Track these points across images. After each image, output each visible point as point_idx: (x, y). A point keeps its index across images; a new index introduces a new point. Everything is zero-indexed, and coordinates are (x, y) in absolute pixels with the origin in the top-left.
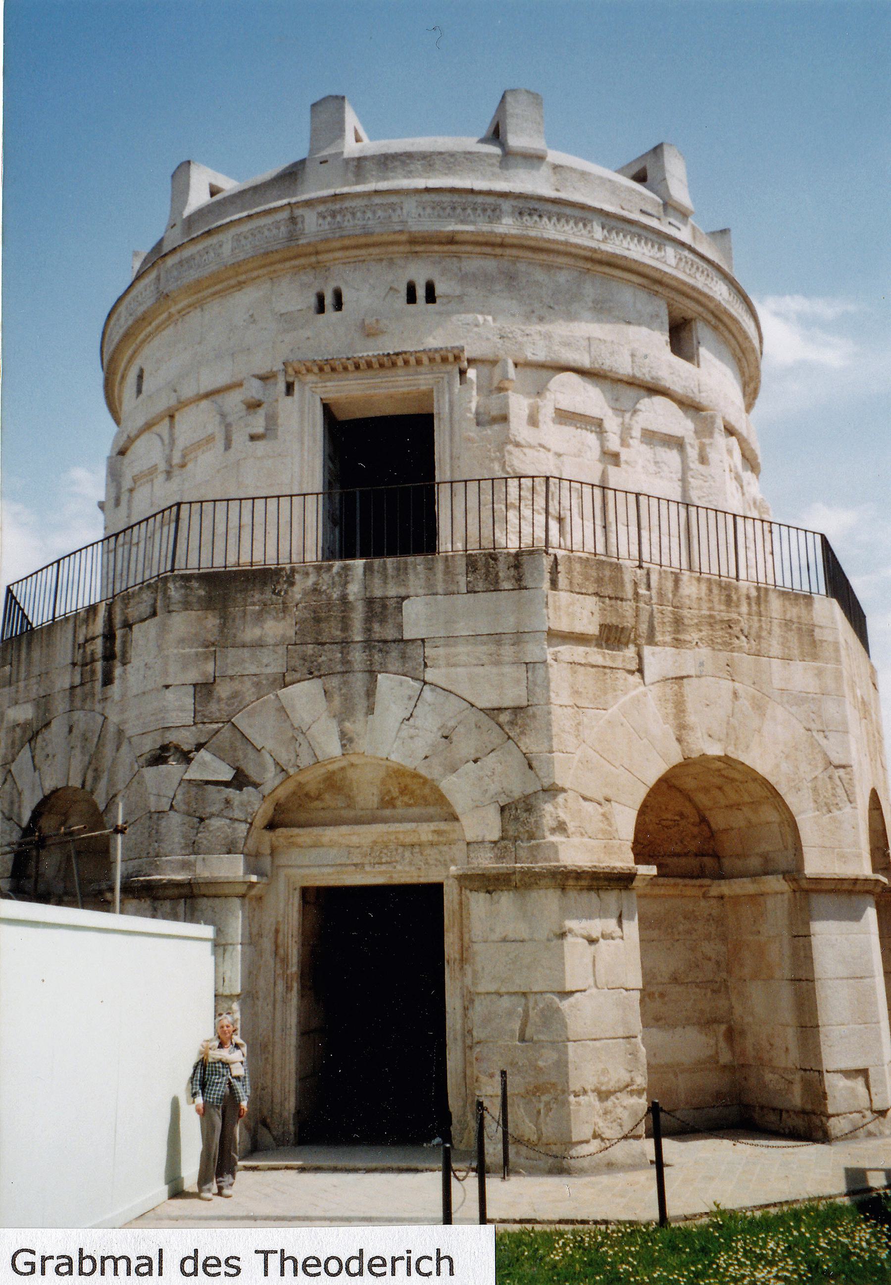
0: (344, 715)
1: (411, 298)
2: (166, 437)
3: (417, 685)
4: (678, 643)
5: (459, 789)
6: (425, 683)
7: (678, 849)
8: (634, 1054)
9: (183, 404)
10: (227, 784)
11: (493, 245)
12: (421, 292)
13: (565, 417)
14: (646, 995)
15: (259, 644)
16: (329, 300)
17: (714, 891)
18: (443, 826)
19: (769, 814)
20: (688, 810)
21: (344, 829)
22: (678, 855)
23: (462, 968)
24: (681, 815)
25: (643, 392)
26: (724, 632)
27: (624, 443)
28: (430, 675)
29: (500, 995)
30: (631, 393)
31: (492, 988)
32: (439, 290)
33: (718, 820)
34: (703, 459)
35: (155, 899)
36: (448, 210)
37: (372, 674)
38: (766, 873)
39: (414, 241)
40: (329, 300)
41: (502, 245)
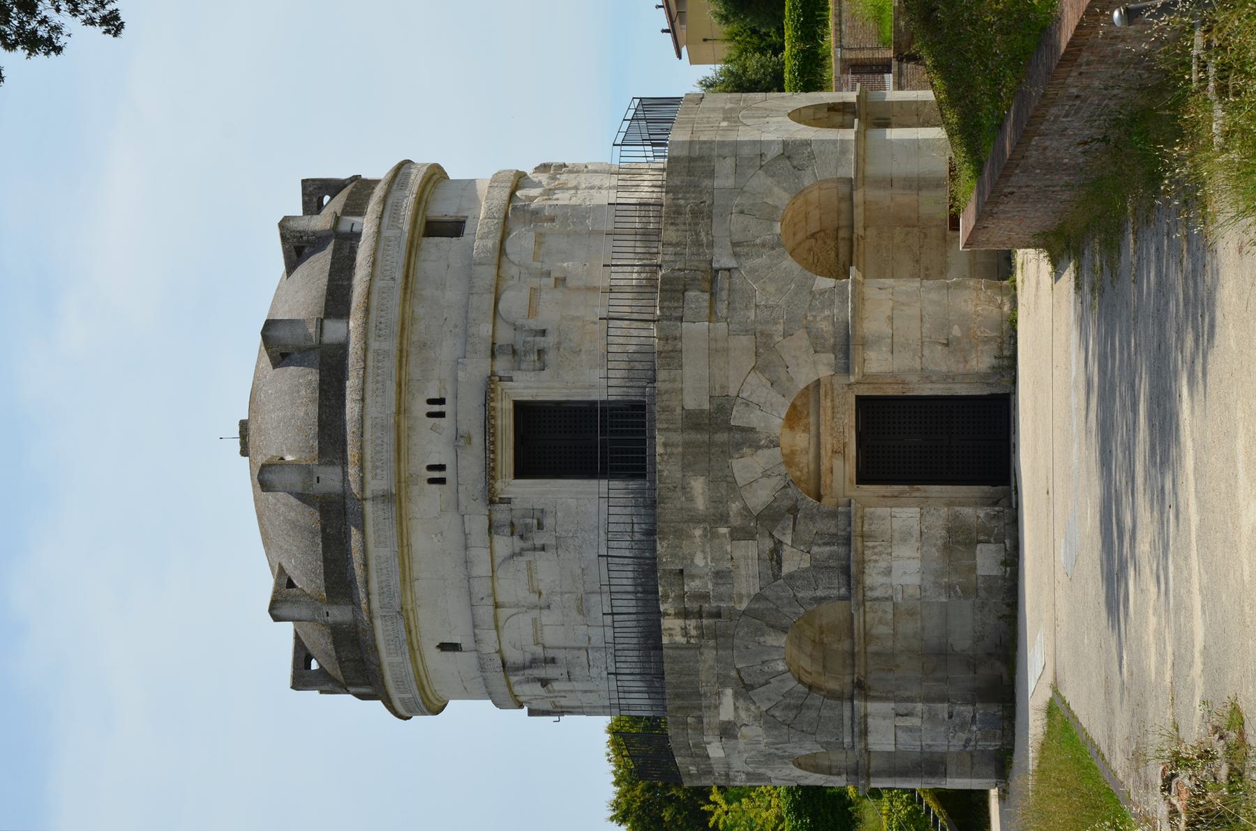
1: (441, 415)
4: (711, 245)
5: (803, 378)
7: (833, 254)
8: (957, 285)
9: (493, 594)
10: (795, 519)
11: (401, 357)
13: (532, 310)
14: (927, 277)
16: (436, 475)
17: (861, 232)
20: (807, 244)
21: (823, 452)
22: (837, 256)
24: (810, 250)
25: (504, 259)
26: (702, 214)
27: (548, 274)
28: (733, 393)
30: (505, 266)
31: (918, 360)
32: (435, 395)
33: (814, 227)
34: (552, 219)
35: (864, 562)
37: (731, 429)
38: (852, 199)
39: (398, 412)
40: (436, 475)
41: (401, 351)
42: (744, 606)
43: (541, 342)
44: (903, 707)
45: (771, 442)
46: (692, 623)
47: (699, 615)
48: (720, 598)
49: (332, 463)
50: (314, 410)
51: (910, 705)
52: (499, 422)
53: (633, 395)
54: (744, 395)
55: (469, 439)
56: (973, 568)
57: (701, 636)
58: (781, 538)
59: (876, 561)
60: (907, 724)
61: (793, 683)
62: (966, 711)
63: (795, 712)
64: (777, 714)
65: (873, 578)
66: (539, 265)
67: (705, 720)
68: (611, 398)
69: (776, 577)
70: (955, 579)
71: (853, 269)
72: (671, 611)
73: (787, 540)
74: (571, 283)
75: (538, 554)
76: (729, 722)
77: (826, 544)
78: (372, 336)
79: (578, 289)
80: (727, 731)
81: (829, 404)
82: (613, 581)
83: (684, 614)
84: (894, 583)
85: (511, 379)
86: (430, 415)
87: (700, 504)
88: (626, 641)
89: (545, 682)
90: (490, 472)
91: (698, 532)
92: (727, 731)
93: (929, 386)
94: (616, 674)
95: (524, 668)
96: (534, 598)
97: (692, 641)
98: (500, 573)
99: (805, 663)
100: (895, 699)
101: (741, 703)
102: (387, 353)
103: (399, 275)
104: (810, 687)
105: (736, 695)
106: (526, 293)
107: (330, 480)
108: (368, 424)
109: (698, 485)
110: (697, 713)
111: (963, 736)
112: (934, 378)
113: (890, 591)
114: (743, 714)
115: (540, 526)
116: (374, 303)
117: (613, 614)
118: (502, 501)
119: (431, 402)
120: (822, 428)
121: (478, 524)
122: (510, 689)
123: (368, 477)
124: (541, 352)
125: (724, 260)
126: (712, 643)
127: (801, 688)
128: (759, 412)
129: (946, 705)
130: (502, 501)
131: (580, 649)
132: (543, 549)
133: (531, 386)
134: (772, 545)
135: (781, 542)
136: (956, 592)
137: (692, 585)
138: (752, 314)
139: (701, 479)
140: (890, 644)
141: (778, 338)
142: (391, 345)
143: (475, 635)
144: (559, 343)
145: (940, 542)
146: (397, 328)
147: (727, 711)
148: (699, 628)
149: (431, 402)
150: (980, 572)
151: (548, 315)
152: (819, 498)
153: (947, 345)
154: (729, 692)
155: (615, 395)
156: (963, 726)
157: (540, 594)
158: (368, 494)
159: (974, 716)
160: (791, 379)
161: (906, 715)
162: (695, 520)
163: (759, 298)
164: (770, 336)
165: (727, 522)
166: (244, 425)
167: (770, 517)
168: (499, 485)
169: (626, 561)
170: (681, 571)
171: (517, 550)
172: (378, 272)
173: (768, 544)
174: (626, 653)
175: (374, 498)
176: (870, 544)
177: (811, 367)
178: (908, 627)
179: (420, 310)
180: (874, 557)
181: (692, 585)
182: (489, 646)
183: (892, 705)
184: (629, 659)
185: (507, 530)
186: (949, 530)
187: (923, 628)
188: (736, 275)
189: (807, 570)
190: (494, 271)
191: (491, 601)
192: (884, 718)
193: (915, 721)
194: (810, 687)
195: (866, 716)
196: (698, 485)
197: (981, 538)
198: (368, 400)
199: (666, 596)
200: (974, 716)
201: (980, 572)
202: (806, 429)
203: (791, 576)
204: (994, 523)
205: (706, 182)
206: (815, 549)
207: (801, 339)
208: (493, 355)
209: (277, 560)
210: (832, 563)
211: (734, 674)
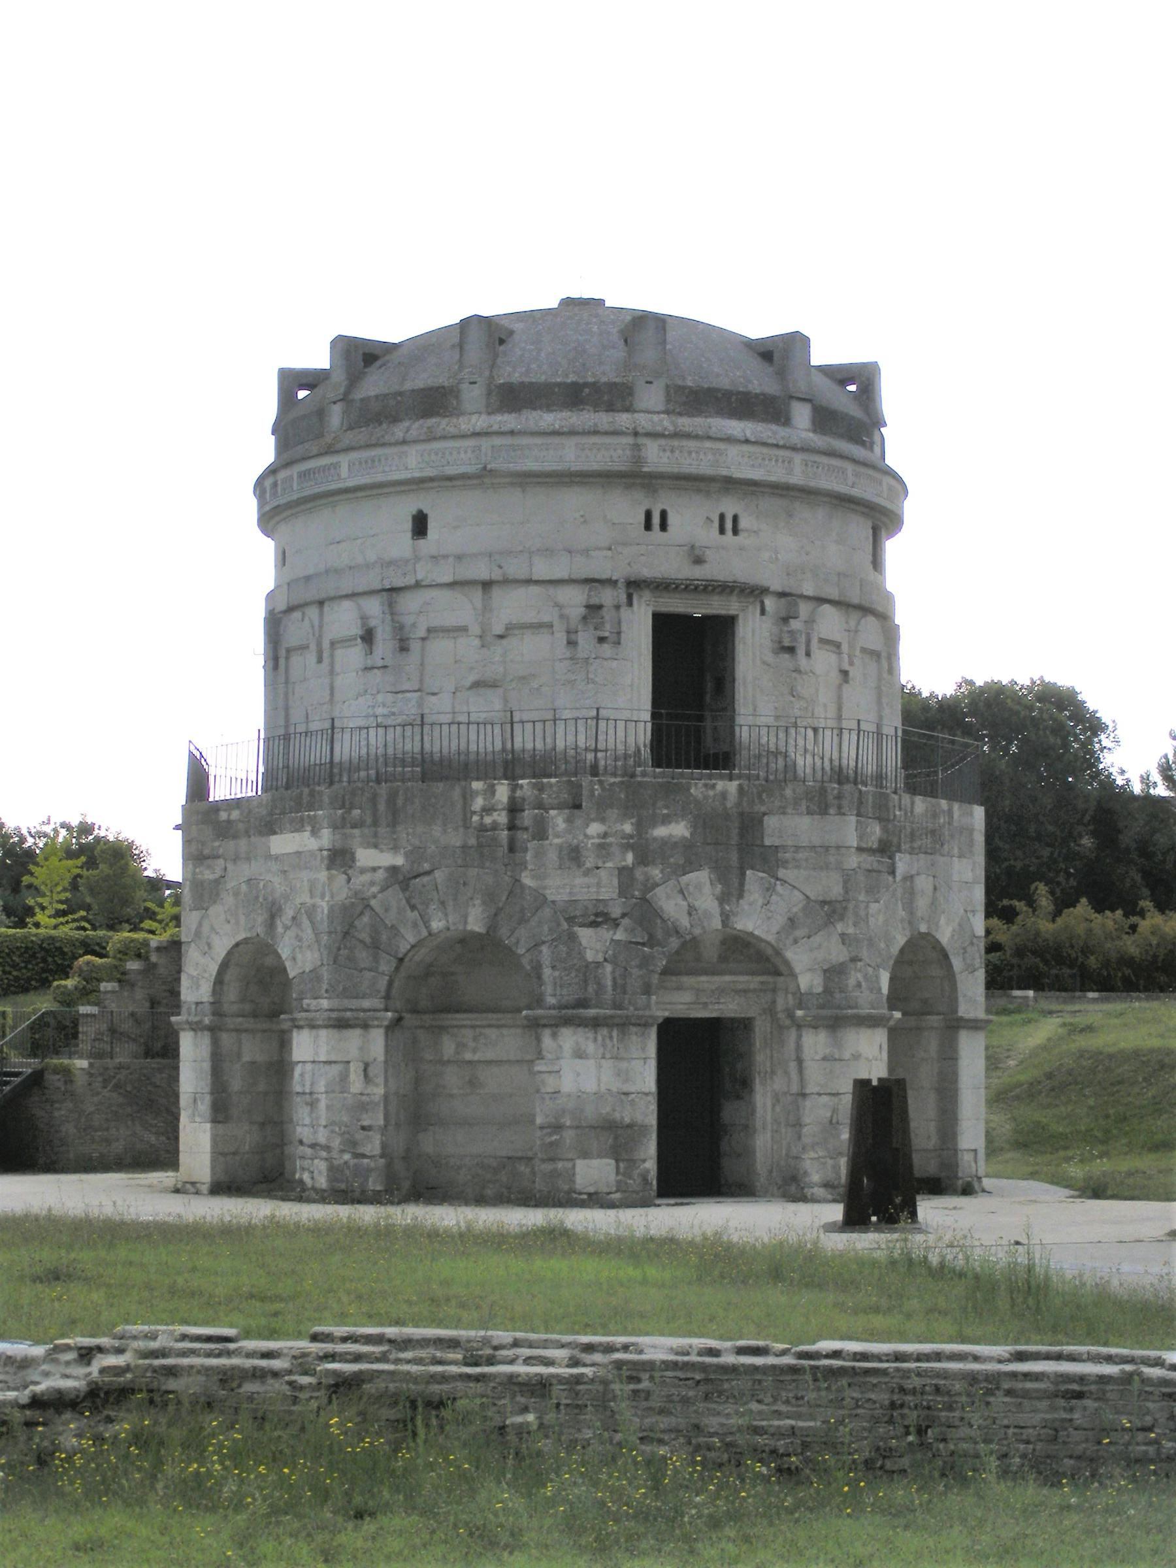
0: (723, 899)
1: (722, 531)
2: (479, 605)
3: (773, 881)
6: (778, 879)
9: (508, 582)
12: (729, 525)
15: (664, 842)
16: (656, 520)
18: (770, 979)
19: (936, 971)
23: (771, 1078)
27: (851, 663)
29: (820, 1094)
31: (816, 1089)
32: (743, 523)
36: (760, 461)
40: (656, 520)
42: (527, 880)
43: (801, 651)
44: (377, 1071)
45: (727, 917)
46: (502, 818)
47: (512, 827)
48: (539, 854)
49: (668, 401)
50: (724, 383)
51: (380, 1080)
52: (716, 598)
53: (742, 758)
54: (779, 888)
55: (699, 561)
56: (585, 1155)
57: (482, 828)
58: (621, 928)
59: (595, 1040)
60: (352, 1077)
61: (412, 940)
62: (373, 1146)
63: (368, 940)
64: (366, 919)
65: (569, 1038)
66: (857, 653)
67: (356, 832)
68: (737, 729)
69: (571, 920)
70: (569, 1136)
71: (897, 1015)
72: (519, 793)
73: (620, 935)
74: (845, 687)
75: (561, 636)
76: (353, 860)
77: (614, 979)
78: (805, 456)
79: (840, 697)
80: (340, 858)
81: (752, 986)
82: (561, 726)
83: (514, 809)
84: (562, 1062)
85: (763, 612)
86: (722, 517)
87: (661, 832)
88: (489, 739)
89: (368, 637)
90: (662, 586)
91: (628, 828)
92: (340, 858)
93: (769, 1104)
94: (333, 728)
95: (392, 614)
96: (498, 629)
97: (475, 818)
98: (535, 590)
99: (421, 955)
100: (386, 1062)
101: (380, 875)
102: (790, 472)
103: (856, 492)
104: (401, 960)
105: (393, 870)
106: (837, 637)
107: (651, 397)
108: (722, 446)
109: (679, 830)
110: (369, 821)
111: (336, 1143)
112: (778, 1109)
113: (549, 1056)
114: (366, 878)
115: (602, 640)
116: (835, 462)
117: (512, 724)
118: (630, 598)
119: (735, 519)
120: (727, 978)
121: (600, 567)
122: (347, 596)
123: (663, 442)
124: (791, 650)
125: (903, 863)
126: (472, 841)
127: (404, 947)
128: (760, 902)
129: (382, 1122)
130: (630, 598)
131: (421, 681)
132: (572, 643)
133: (753, 638)
134: (613, 916)
135: (618, 925)
136: (550, 1135)
137: (558, 820)
138: (862, 897)
139: (687, 834)
140: (428, 1057)
141: (840, 927)
142: (797, 478)
143: (446, 557)
144: (800, 672)
145: (617, 1116)
146: (812, 484)
147: (366, 857)
148: (495, 827)
149: (735, 519)
150: (580, 1164)
151: (823, 662)
152: (665, 972)
153: (831, 1122)
154: (399, 861)
155: (743, 734)
156: (351, 1144)
157: (501, 637)
158: (642, 440)
159: (364, 1156)
160: (796, 941)
161: (366, 1075)
162: (640, 827)
163: (874, 907)
164: (842, 918)
165: (639, 863)
166: (601, 302)
167: (645, 913)
168: (647, 595)
169: (549, 740)
170: (578, 806)
171: (566, 611)
172: (862, 469)
173: (616, 912)
174: (417, 738)
175: (637, 447)
176: (615, 1033)
177: (806, 965)
178: (452, 1079)
179: (821, 513)
180: (600, 1038)
181: (558, 820)
182: (422, 572)
183: (381, 1058)
184: (408, 740)
185: (595, 601)
186: (630, 1126)
187: (452, 1096)
188: (891, 878)
189: (581, 956)
190: (855, 600)
191: (494, 577)
192: (361, 1049)
193: (356, 1083)
194: (401, 960)
195: (313, 1027)
196: (679, 830)
197: (621, 1165)
198: (746, 448)
199: (541, 788)
200: (364, 1156)
201: (580, 1164)
202: (723, 959)
203: (573, 937)
204: (639, 1181)
205: (956, 851)
206: (609, 968)
207: (837, 953)
208: (782, 595)
209: (517, 326)
210: (591, 988)
211: (426, 866)
